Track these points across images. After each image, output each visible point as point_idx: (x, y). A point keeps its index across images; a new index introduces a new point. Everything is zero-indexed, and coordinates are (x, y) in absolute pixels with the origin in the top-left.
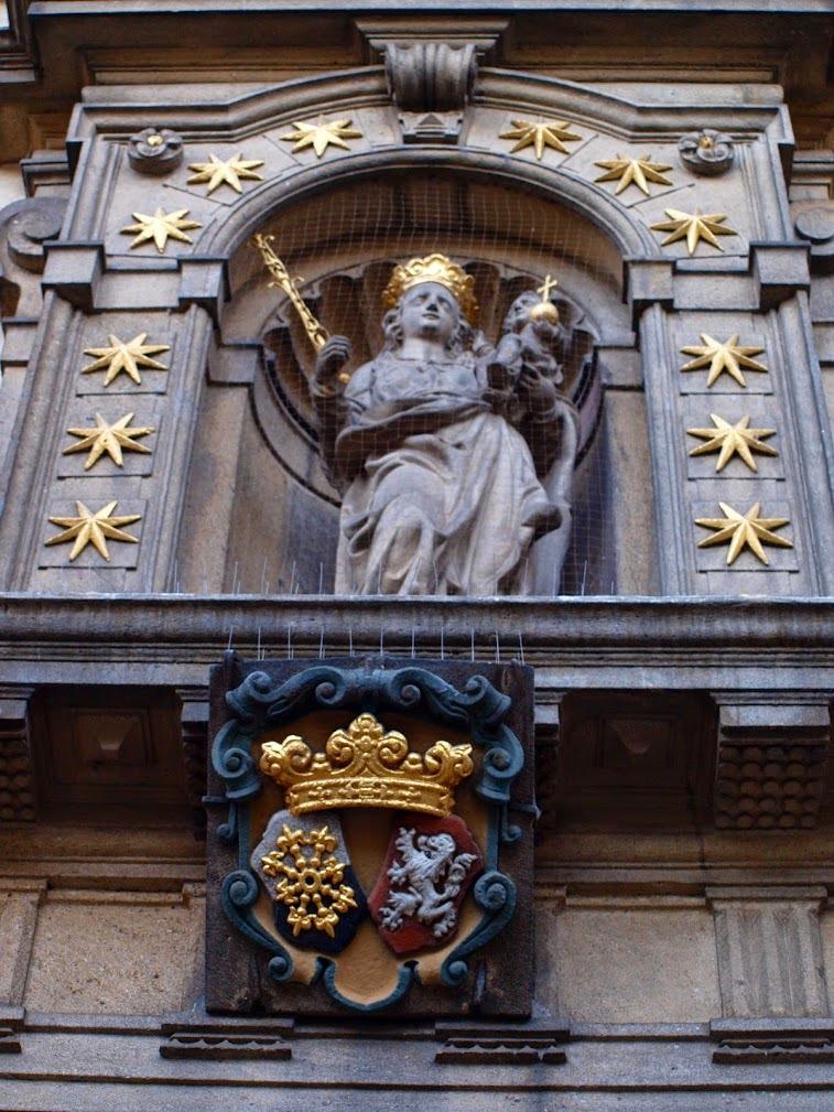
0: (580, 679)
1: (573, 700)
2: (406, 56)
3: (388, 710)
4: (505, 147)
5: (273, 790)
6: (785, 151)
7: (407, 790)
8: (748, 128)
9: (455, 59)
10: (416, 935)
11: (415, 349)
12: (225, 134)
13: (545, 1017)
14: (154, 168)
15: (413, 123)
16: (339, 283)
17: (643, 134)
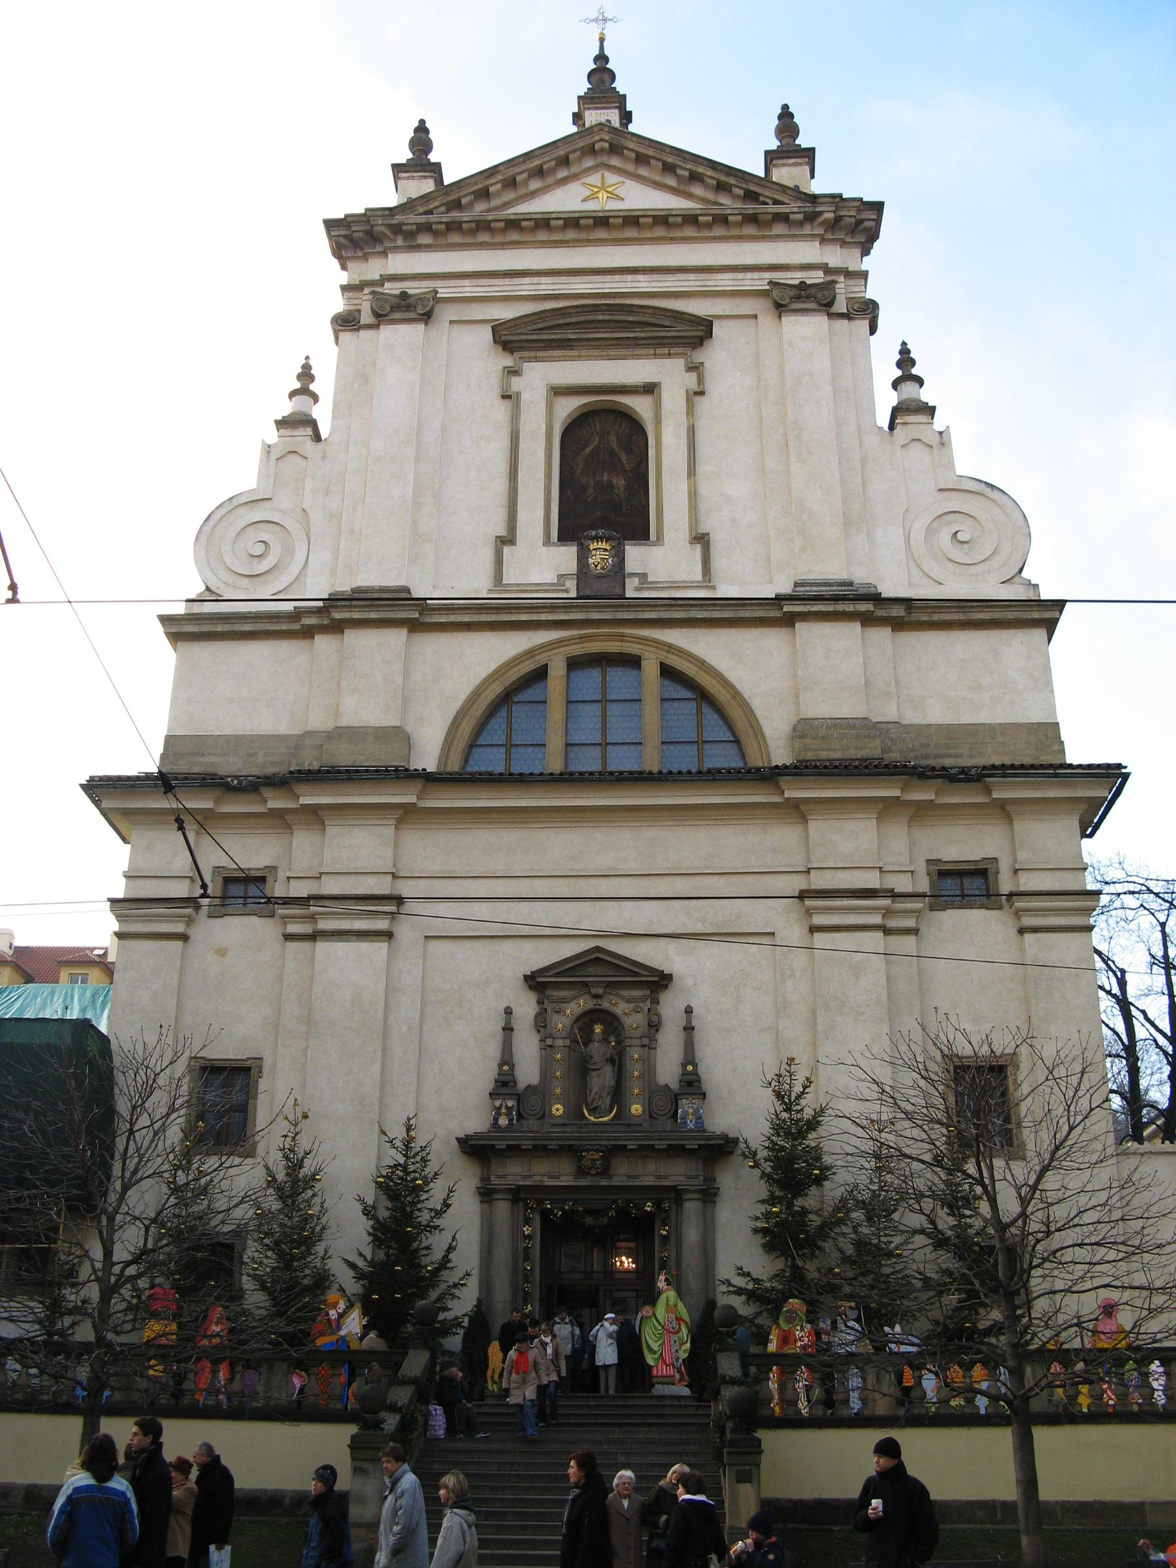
0: (614, 1143)
1: (613, 1145)
2: (593, 991)
3: (594, 1151)
4: (608, 1005)
5: (584, 1157)
6: (649, 1010)
7: (598, 1157)
8: (643, 999)
9: (600, 991)
10: (598, 1168)
11: (596, 1044)
12: (567, 1002)
13: (610, 1173)
14: (557, 1012)
15: (595, 1001)
16: (585, 1023)
17: (629, 1001)
